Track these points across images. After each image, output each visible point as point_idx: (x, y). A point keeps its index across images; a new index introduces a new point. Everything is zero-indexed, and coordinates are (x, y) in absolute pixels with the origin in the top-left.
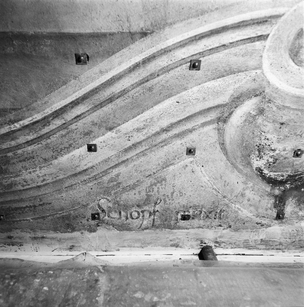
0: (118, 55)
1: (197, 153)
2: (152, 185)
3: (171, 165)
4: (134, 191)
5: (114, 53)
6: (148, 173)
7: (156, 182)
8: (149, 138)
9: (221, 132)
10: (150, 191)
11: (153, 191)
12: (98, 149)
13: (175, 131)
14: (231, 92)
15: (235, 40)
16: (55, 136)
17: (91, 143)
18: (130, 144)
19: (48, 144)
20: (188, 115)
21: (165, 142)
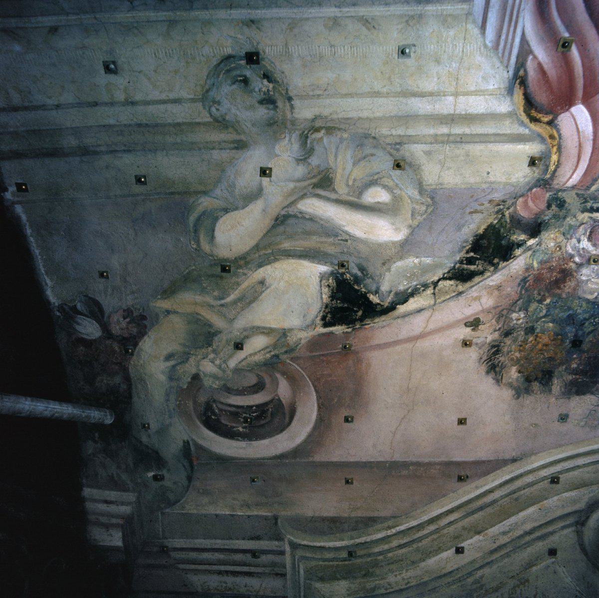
0: (491, 475)
1: (559, 553)
2: (514, 587)
3: (534, 565)
4: (497, 594)
5: (489, 474)
6: (511, 574)
7: (519, 583)
8: (513, 540)
9: (579, 534)
10: (512, 594)
11: (516, 593)
12: (466, 551)
13: (538, 534)
14: (586, 500)
15: (586, 462)
16: (426, 540)
17: (459, 546)
18: (495, 546)
19: (418, 547)
20: (549, 519)
21: (528, 544)
